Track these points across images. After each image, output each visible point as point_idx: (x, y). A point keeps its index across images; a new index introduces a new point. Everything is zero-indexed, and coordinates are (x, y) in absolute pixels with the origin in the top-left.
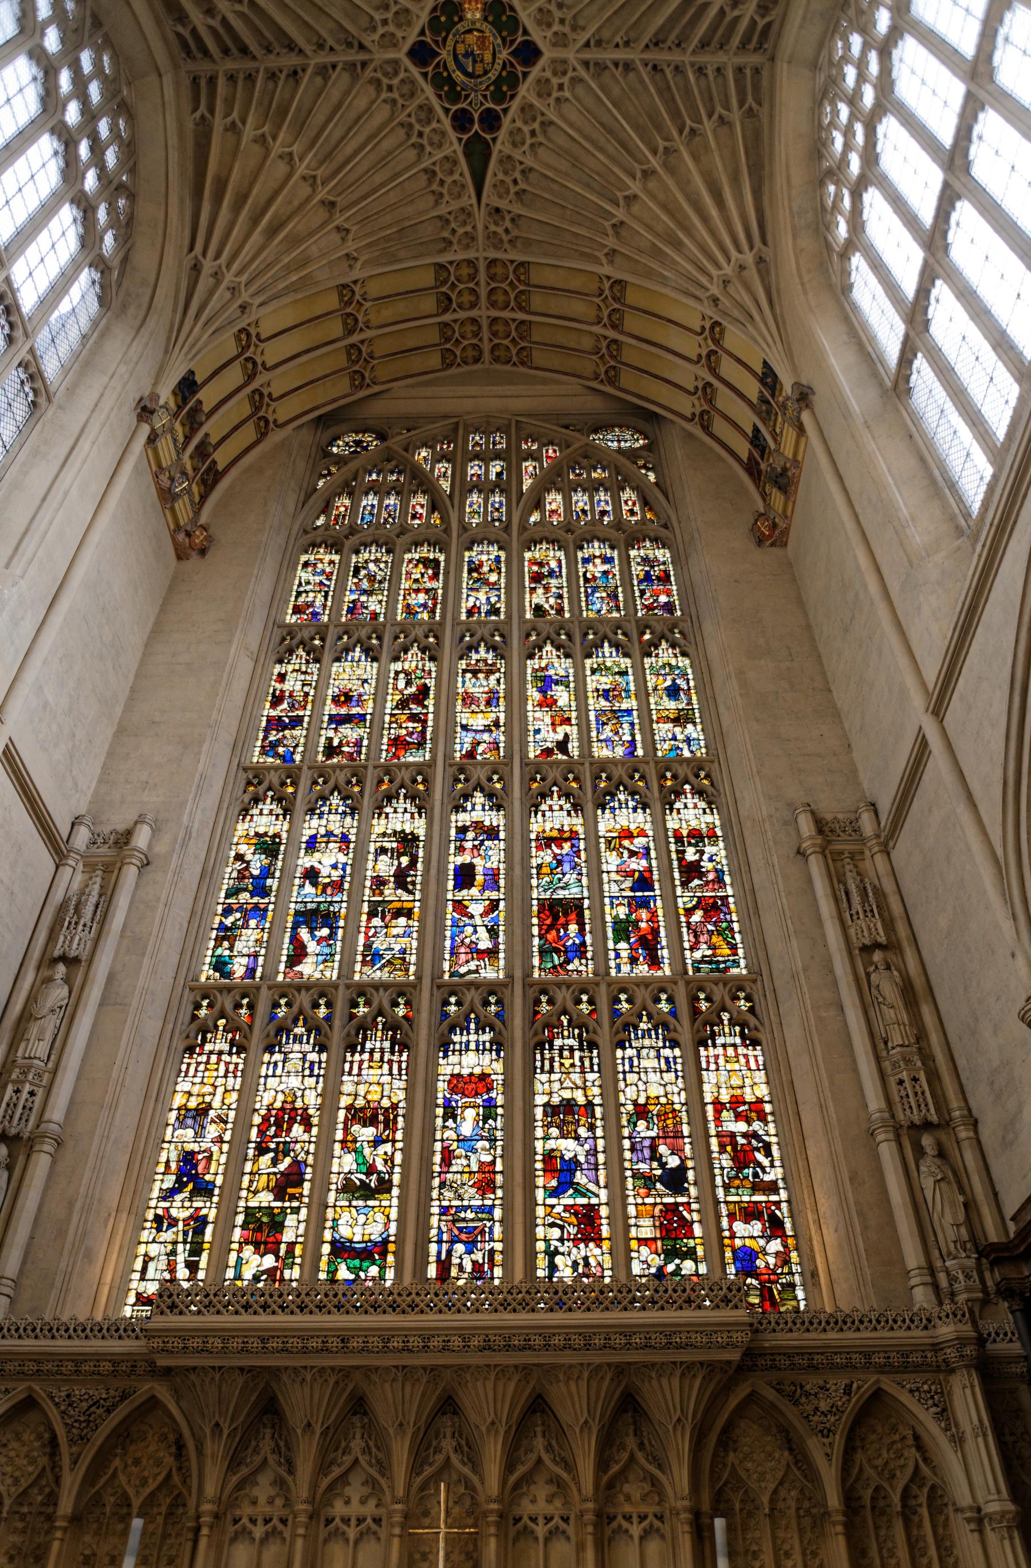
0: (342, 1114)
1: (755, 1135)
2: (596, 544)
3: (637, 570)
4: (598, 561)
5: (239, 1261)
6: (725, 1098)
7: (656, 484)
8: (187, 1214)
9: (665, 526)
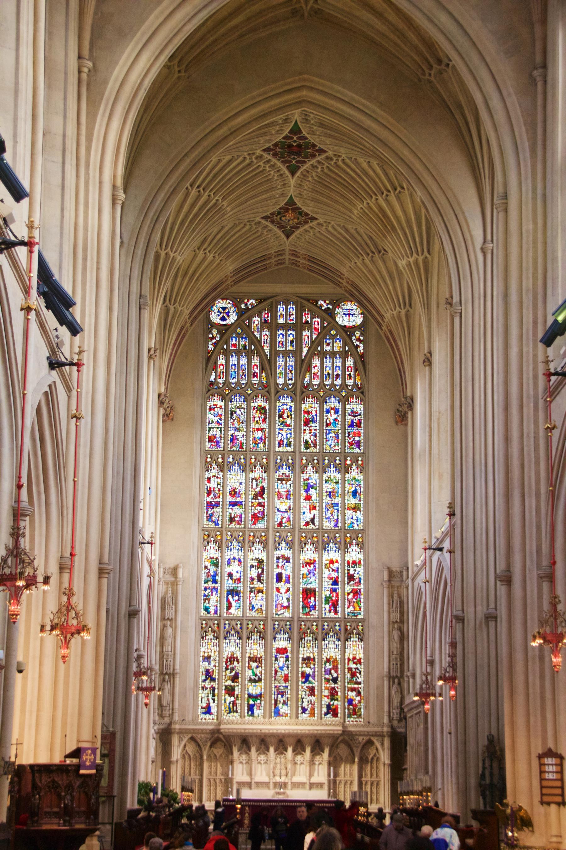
0: (247, 659)
1: (358, 669)
2: (333, 399)
3: (349, 419)
4: (332, 412)
5: (225, 700)
6: (351, 657)
7: (362, 356)
8: (210, 686)
9: (362, 393)
